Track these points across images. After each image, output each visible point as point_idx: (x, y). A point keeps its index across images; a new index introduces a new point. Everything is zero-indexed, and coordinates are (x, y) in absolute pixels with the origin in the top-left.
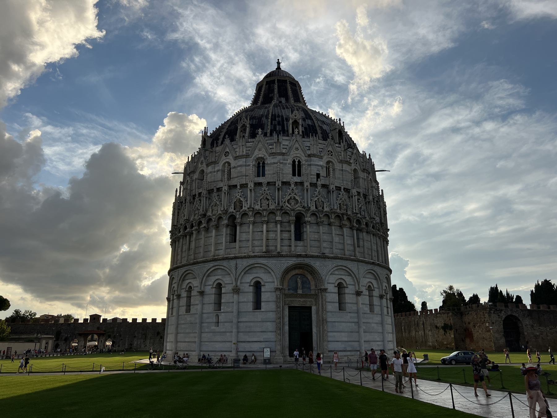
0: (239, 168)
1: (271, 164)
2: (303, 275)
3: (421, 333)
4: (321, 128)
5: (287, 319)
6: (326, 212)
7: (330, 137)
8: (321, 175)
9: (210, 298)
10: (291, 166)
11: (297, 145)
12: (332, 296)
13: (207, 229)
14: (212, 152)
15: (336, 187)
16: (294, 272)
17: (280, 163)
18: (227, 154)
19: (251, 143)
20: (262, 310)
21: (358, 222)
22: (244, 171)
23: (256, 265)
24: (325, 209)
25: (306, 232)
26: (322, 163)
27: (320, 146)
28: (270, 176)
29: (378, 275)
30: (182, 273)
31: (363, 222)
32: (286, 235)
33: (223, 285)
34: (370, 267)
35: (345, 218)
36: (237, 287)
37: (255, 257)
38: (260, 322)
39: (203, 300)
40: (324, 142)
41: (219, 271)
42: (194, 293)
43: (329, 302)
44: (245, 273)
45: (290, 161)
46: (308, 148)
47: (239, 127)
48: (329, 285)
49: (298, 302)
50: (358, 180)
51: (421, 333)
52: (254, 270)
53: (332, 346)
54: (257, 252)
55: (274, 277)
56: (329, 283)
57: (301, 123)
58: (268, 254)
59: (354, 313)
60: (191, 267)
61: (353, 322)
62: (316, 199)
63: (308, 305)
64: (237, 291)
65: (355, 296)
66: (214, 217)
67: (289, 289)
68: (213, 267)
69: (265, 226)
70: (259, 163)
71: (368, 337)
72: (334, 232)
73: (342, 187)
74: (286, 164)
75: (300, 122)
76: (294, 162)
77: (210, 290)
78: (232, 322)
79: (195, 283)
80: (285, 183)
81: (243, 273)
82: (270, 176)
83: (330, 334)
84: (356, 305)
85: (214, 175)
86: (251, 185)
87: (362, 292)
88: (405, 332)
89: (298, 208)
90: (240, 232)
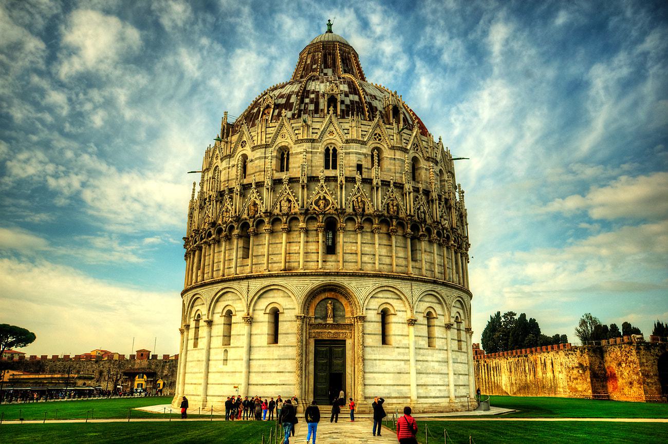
0: (256, 162)
1: (297, 154)
2: (335, 300)
3: (549, 375)
4: (370, 104)
5: (311, 357)
7: (378, 117)
8: (363, 166)
9: (219, 329)
10: (322, 156)
12: (374, 327)
13: (218, 242)
14: (227, 142)
15: (381, 181)
16: (323, 296)
17: (307, 152)
18: (243, 144)
19: (272, 129)
20: (279, 344)
21: (415, 228)
22: (262, 165)
23: (272, 287)
24: (367, 212)
25: (339, 242)
26: (366, 150)
27: (364, 128)
30: (191, 297)
31: (422, 228)
32: (312, 247)
34: (429, 287)
36: (248, 314)
37: (271, 276)
38: (276, 359)
39: (210, 332)
41: (229, 294)
42: (202, 323)
43: (369, 334)
44: (259, 298)
45: (321, 148)
46: (346, 131)
48: (369, 311)
50: (419, 171)
51: (549, 375)
52: (271, 294)
54: (277, 270)
55: (295, 301)
56: (370, 309)
57: (339, 99)
58: (288, 272)
59: (404, 348)
60: (198, 290)
61: (403, 360)
62: (354, 198)
63: (341, 337)
65: (406, 326)
66: (225, 226)
67: (316, 318)
68: (222, 289)
69: (284, 235)
70: (283, 154)
71: (424, 379)
72: (377, 242)
74: (316, 153)
75: (339, 98)
76: (327, 150)
77: (219, 320)
78: (242, 360)
80: (313, 179)
81: (256, 298)
82: (296, 168)
83: (367, 376)
84: (407, 338)
85: (229, 172)
86: (268, 182)
87: (415, 321)
88: (530, 375)
90: (254, 245)
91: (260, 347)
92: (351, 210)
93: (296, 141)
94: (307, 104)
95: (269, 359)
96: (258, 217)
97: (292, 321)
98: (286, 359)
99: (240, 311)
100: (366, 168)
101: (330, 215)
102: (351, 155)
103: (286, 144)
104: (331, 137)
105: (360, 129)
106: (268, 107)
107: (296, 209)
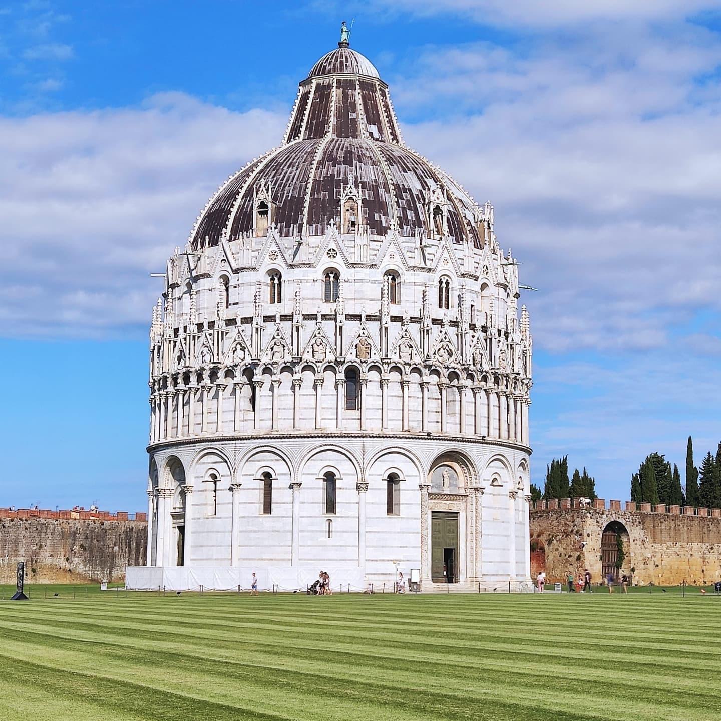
10: (437, 290)
18: (332, 253)
26: (477, 286)
27: (477, 258)
28: (408, 306)
33: (338, 476)
38: (398, 533)
47: (342, 202)
49: (443, 506)
53: (486, 568)
64: (361, 487)
68: (321, 446)
76: (441, 282)
79: (279, 468)
81: (373, 460)
89: (452, 363)
91: (378, 518)
92: (472, 365)
95: (390, 532)
96: (373, 362)
97: (414, 490)
98: (409, 533)
99: (349, 474)
100: (478, 311)
101: (453, 370)
103: (396, 268)
104: (446, 267)
107: (417, 359)
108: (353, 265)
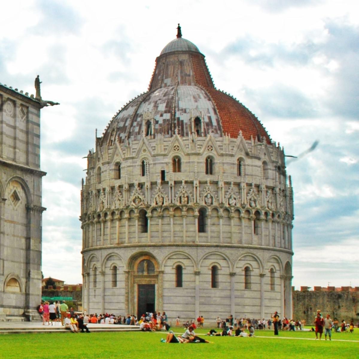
1: (124, 167)
6: (166, 206)
7: (176, 133)
8: (166, 171)
11: (145, 148)
27: (165, 144)
29: (226, 256)
31: (208, 209)
35: (185, 209)
40: (170, 139)
45: (139, 163)
46: (153, 148)
70: (119, 166)
73: (183, 181)
74: (135, 166)
76: (143, 162)
93: (124, 158)
94: (134, 127)
102: (157, 165)
105: (163, 146)
106: (114, 130)
108: (103, 164)
